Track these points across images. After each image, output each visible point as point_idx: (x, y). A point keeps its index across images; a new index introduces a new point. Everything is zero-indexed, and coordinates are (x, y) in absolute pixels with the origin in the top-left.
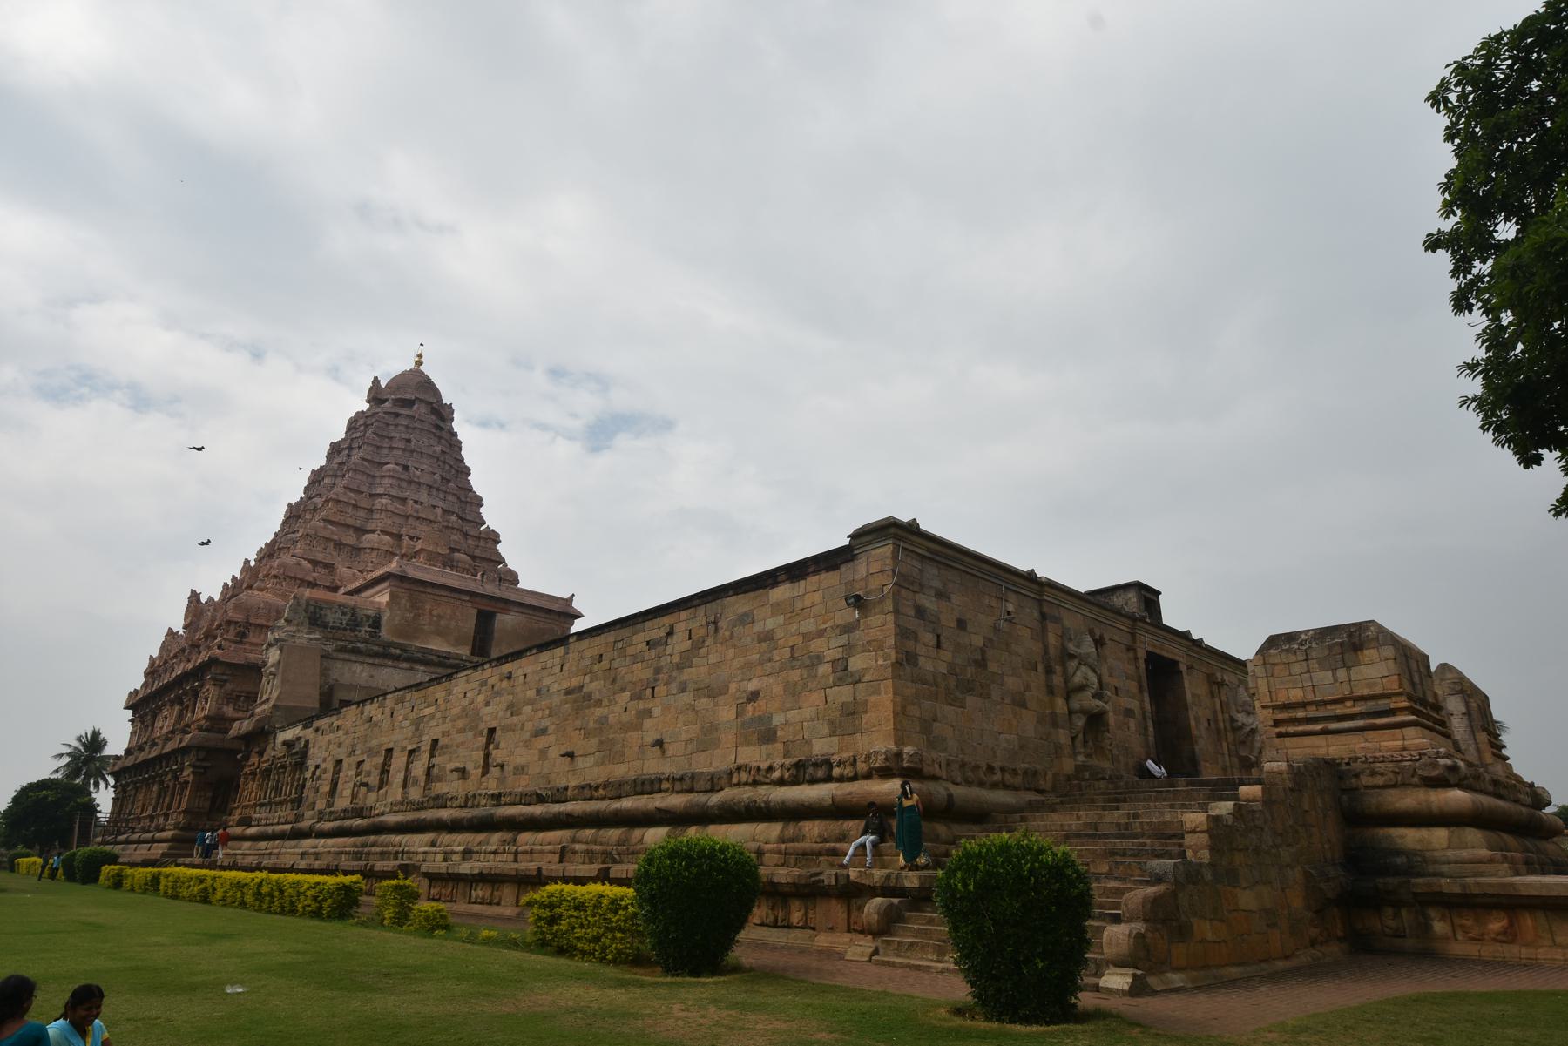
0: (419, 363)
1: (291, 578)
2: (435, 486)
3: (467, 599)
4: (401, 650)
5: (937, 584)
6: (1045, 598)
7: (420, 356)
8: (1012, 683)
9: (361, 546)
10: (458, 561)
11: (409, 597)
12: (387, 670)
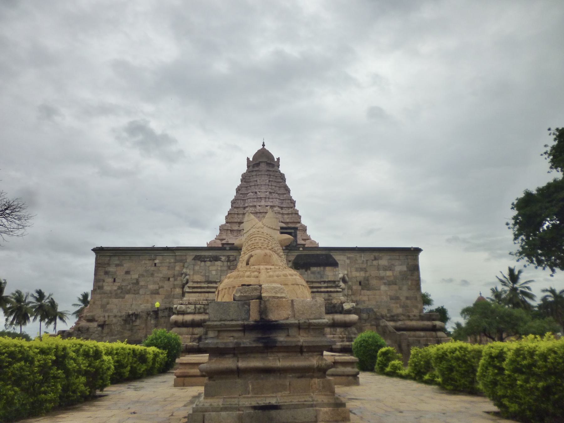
0: (264, 145)
2: (267, 197)
5: (118, 262)
6: (176, 254)
7: (264, 143)
8: (152, 287)
9: (240, 229)
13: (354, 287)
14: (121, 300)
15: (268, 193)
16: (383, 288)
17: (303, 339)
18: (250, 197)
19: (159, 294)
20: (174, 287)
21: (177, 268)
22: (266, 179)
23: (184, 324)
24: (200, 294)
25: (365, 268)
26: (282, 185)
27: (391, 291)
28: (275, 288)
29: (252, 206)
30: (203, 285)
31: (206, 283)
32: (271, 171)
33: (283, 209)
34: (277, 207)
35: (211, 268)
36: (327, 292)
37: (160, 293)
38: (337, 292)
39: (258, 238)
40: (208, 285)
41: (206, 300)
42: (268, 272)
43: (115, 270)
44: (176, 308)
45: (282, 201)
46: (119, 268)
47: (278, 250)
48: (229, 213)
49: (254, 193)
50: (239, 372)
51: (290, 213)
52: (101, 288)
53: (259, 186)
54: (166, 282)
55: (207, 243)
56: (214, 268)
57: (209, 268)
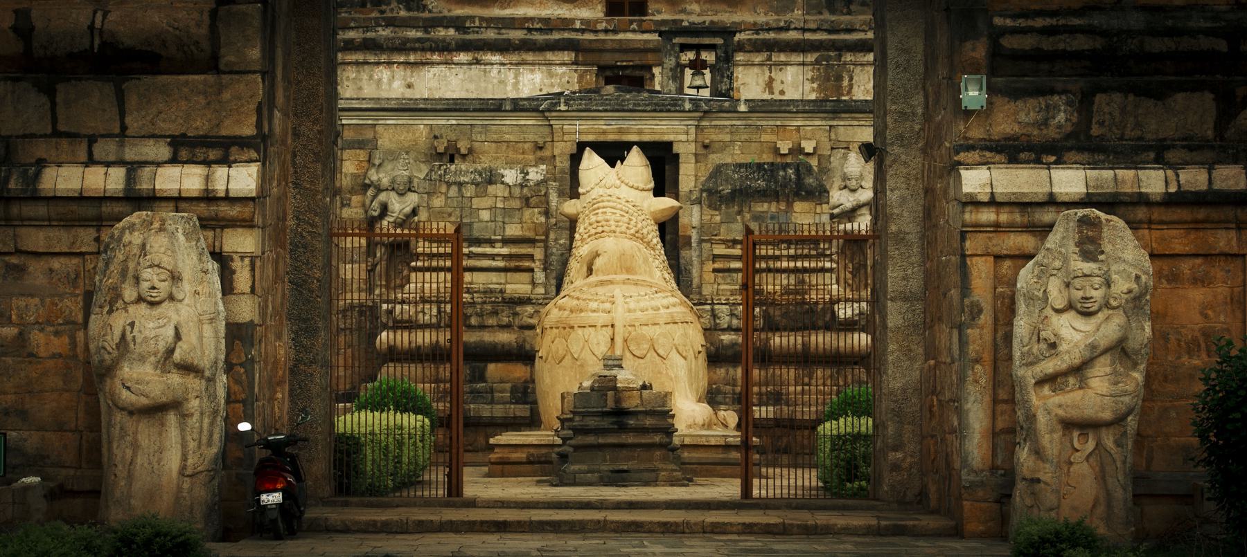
4: (458, 29)
12: (435, 70)
17: (649, 422)
23: (415, 355)
28: (628, 379)
35: (476, 203)
36: (796, 270)
38: (823, 270)
39: (609, 210)
40: (471, 249)
42: (626, 303)
44: (390, 312)
50: (600, 447)
56: (487, 202)
57: (471, 201)
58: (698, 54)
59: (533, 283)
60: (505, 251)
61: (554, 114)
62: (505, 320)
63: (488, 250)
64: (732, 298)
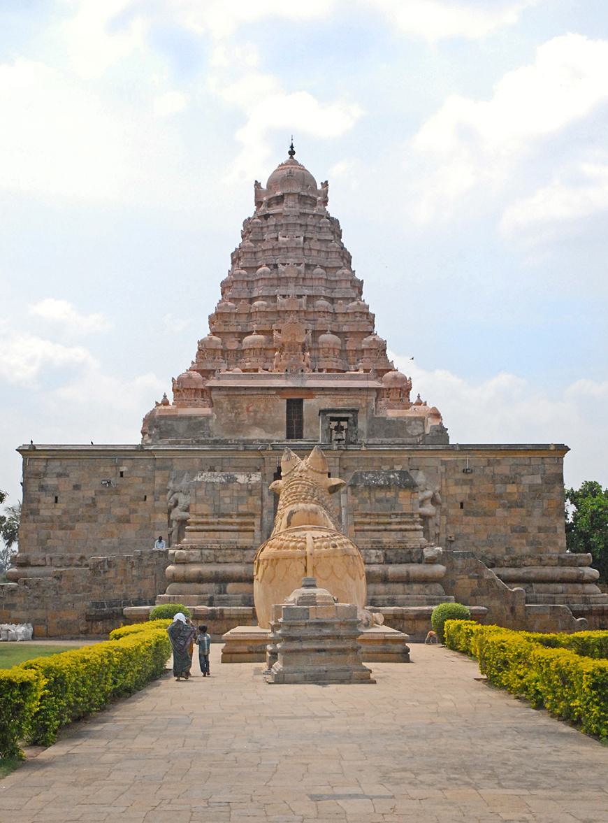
0: (292, 153)
1: (188, 389)
3: (274, 393)
5: (59, 470)
6: (156, 457)
7: (292, 147)
8: (117, 511)
9: (243, 348)
10: (323, 343)
11: (229, 401)
13: (452, 512)
14: (69, 532)
15: (302, 268)
16: (500, 512)
17: (343, 631)
18: (263, 276)
19: (130, 523)
20: (155, 510)
21: (159, 480)
22: (298, 233)
23: (186, 580)
24: (207, 534)
25: (471, 480)
26: (334, 247)
27: (516, 517)
28: (324, 596)
29: (265, 298)
30: (211, 520)
31: (217, 516)
32: (309, 214)
33: (335, 301)
34: (322, 298)
35: (223, 493)
36: (401, 530)
37: (131, 521)
38: (416, 530)
39: (300, 486)
41: (218, 543)
42: (315, 542)
43: (56, 483)
44: (174, 554)
45: (334, 285)
46: (62, 479)
47: (326, 500)
48: (220, 311)
49: (272, 267)
51: (348, 311)
52: (35, 512)
53: (282, 251)
54: (141, 503)
55: (173, 379)
56: (228, 493)
58: (339, 423)
59: (254, 538)
60: (238, 520)
61: (266, 452)
62: (238, 559)
63: (229, 520)
64: (366, 545)
